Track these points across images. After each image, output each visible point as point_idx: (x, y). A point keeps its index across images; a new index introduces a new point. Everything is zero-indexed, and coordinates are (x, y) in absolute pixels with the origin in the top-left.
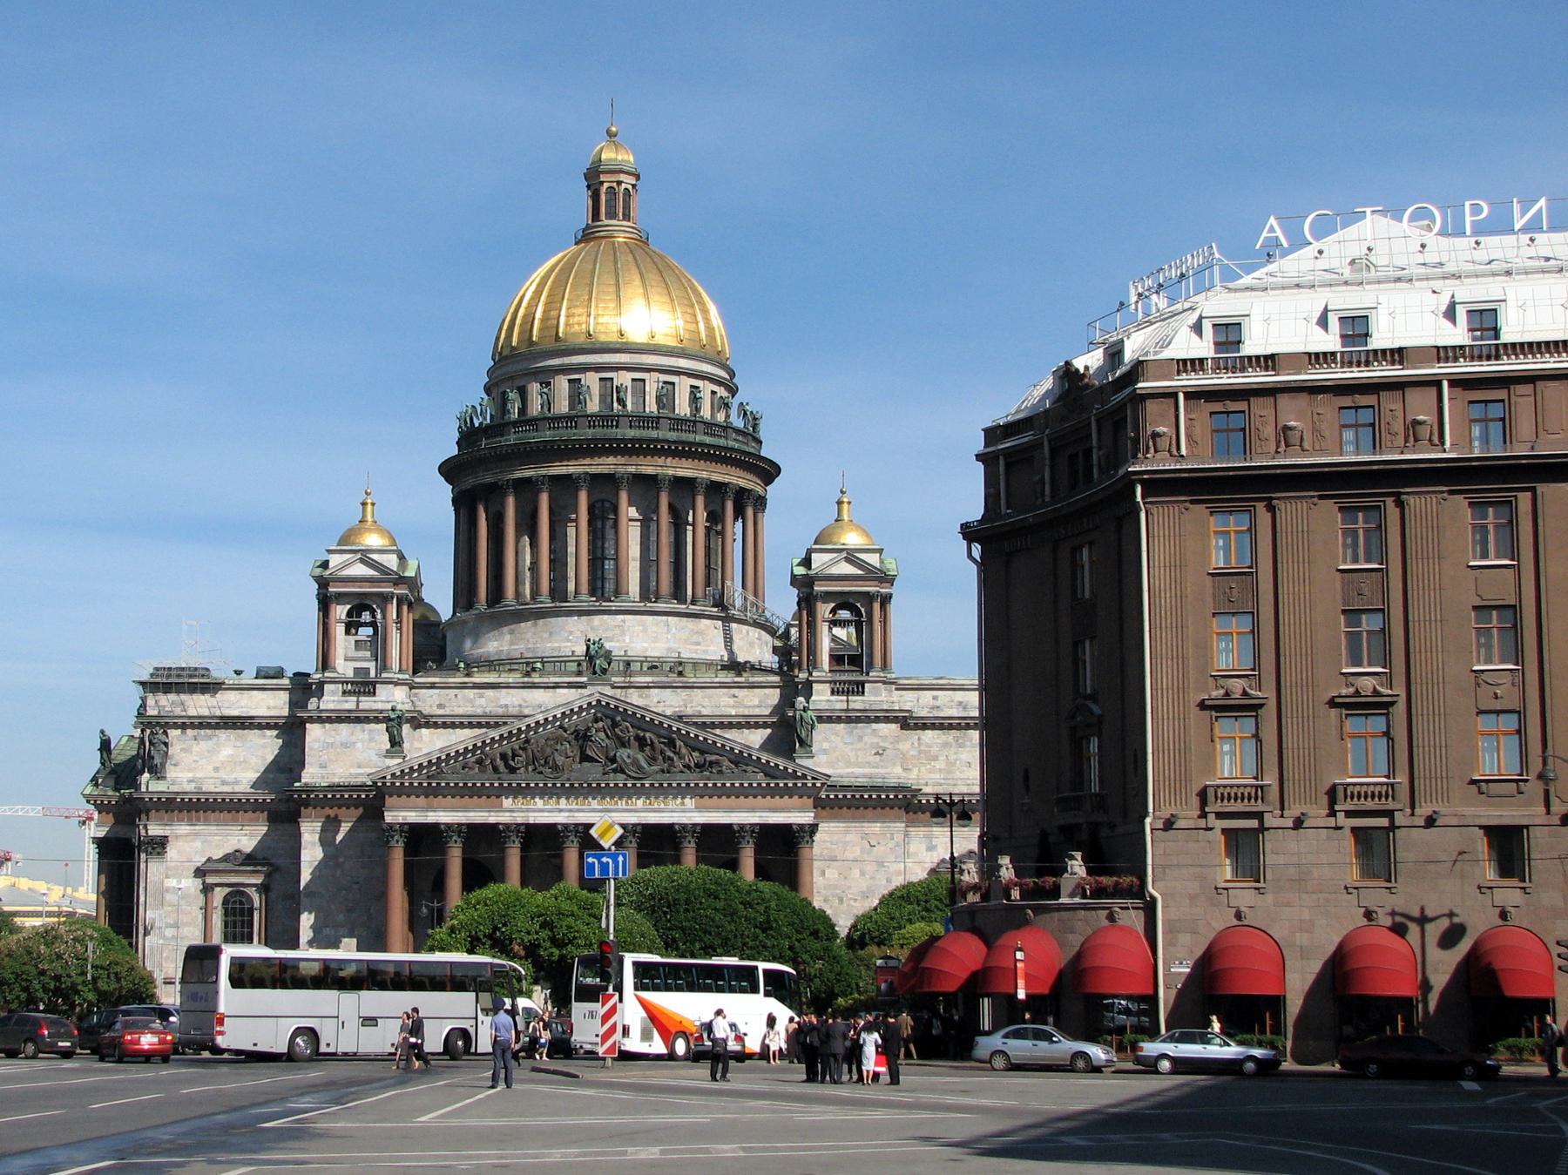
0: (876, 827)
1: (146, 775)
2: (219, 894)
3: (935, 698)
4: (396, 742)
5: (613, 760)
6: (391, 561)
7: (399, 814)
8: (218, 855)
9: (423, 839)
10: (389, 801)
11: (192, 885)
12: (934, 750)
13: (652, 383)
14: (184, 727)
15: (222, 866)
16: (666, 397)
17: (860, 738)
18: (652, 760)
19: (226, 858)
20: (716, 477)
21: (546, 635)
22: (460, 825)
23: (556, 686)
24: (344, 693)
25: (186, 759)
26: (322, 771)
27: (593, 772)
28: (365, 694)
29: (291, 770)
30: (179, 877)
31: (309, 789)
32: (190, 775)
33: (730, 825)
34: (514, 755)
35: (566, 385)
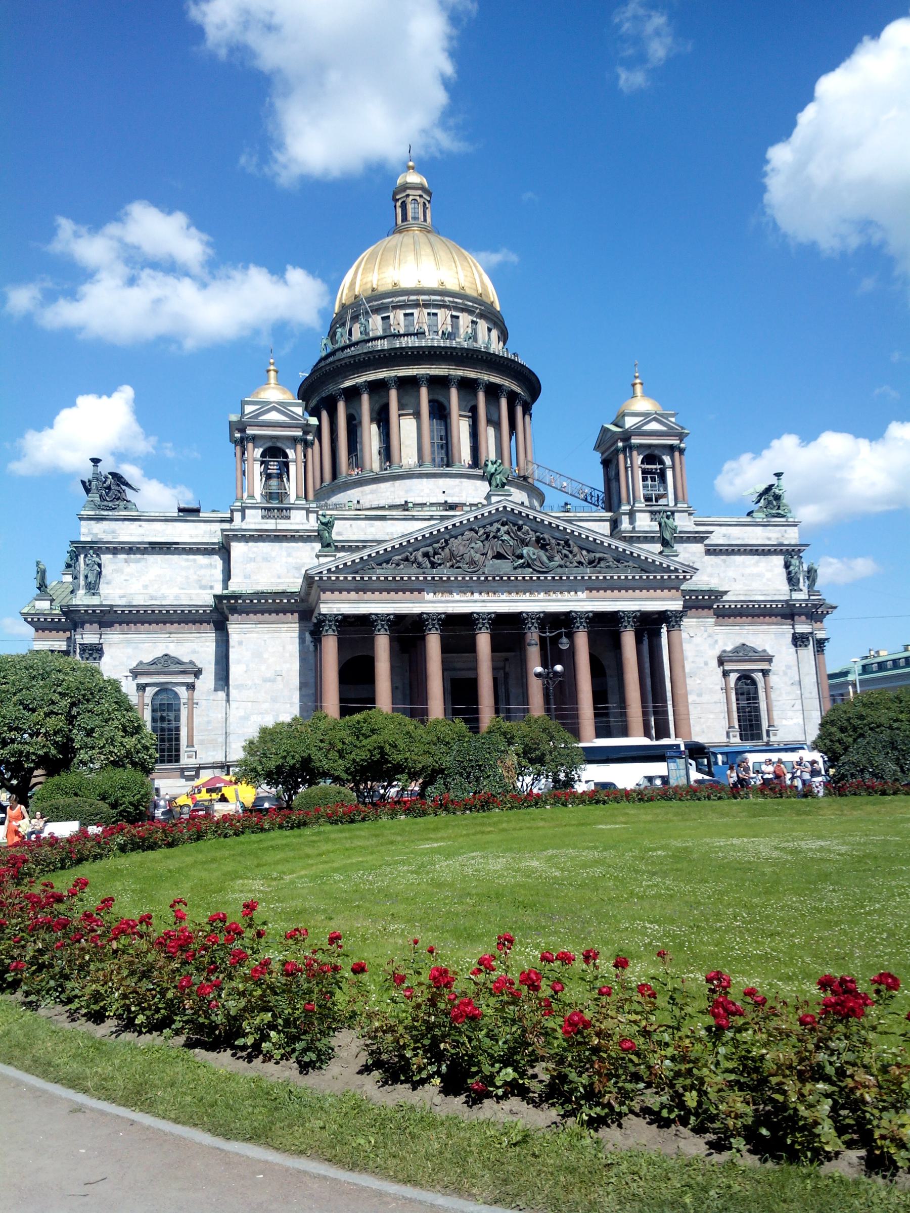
1: (82, 592)
2: (150, 691)
5: (521, 557)
7: (334, 606)
8: (148, 659)
9: (356, 628)
10: (323, 596)
14: (115, 551)
18: (551, 559)
22: (388, 615)
23: (431, 518)
24: (263, 517)
25: (118, 579)
26: (247, 581)
27: (505, 567)
28: (282, 518)
29: (212, 588)
31: (236, 597)
32: (122, 592)
33: (618, 612)
35: (402, 317)
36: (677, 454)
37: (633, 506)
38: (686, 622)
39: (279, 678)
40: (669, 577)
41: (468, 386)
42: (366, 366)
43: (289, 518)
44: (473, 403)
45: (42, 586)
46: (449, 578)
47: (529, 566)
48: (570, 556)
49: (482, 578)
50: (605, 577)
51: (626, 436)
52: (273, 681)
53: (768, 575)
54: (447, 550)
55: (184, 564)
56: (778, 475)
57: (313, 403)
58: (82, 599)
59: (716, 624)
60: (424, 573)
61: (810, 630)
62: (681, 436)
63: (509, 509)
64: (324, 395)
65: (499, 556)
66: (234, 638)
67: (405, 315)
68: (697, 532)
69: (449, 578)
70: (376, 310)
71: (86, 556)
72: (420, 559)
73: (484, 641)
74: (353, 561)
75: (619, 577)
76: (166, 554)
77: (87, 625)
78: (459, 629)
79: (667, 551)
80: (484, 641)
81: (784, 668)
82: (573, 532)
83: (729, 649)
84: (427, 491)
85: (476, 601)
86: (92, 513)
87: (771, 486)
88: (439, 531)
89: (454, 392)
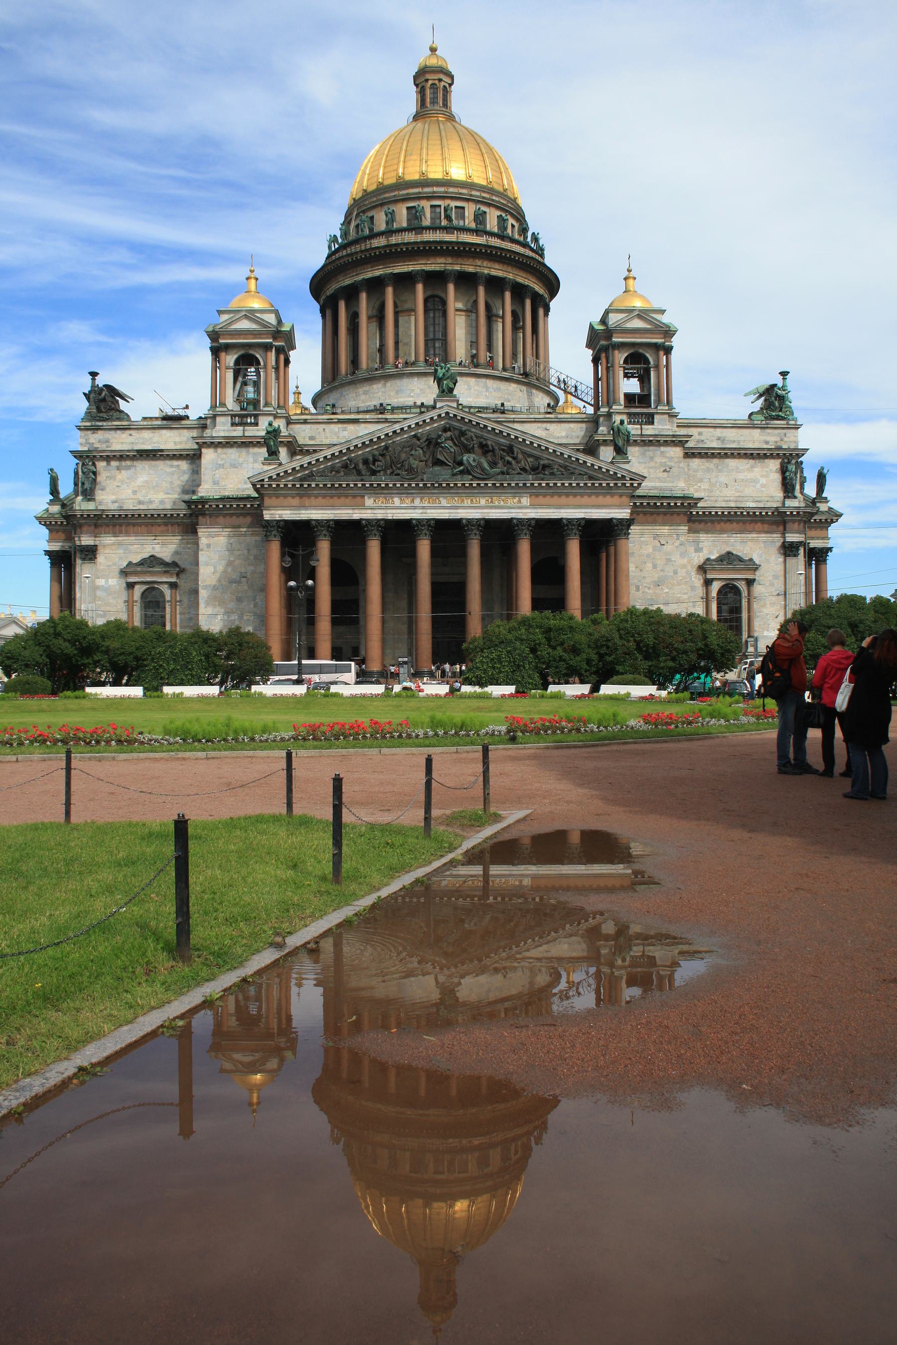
0: (665, 530)
1: (80, 498)
2: (138, 590)
3: (700, 434)
4: (273, 454)
5: (460, 463)
6: (271, 319)
7: (276, 513)
8: (136, 559)
10: (267, 501)
11: (115, 583)
12: (700, 474)
13: (470, 210)
14: (108, 459)
15: (139, 569)
16: (480, 218)
17: (652, 458)
18: (493, 464)
19: (142, 563)
20: (520, 280)
21: (393, 394)
22: (328, 521)
24: (233, 424)
25: (110, 485)
26: (216, 487)
28: (251, 424)
29: (194, 492)
30: (107, 577)
31: (203, 501)
32: (114, 497)
34: (375, 460)
35: (405, 212)
36: (661, 353)
37: (611, 408)
38: (634, 529)
39: (244, 580)
40: (616, 484)
41: (466, 281)
42: (363, 264)
43: (256, 424)
44: (474, 298)
45: (54, 491)
46: (387, 485)
47: (469, 473)
48: (513, 462)
49: (421, 485)
50: (547, 484)
51: (608, 333)
52: (238, 582)
53: (763, 481)
54: (388, 457)
55: (169, 470)
56: (784, 374)
57: (322, 302)
58: (81, 505)
59: (690, 531)
60: (362, 480)
61: (803, 539)
62: (669, 332)
63: (451, 415)
64: (328, 294)
65: (438, 463)
66: (203, 541)
67: (408, 208)
68: (674, 436)
69: (387, 485)
70: (382, 205)
71: (83, 464)
72: (361, 466)
73: (424, 548)
74: (294, 469)
75: (563, 484)
76: (152, 460)
77: (85, 528)
78: (398, 534)
79: (619, 459)
80: (424, 548)
81: (771, 578)
82: (516, 437)
83: (713, 557)
84: (418, 391)
85: (415, 508)
86: (88, 424)
87: (774, 386)
88: (379, 438)
89: (451, 287)
